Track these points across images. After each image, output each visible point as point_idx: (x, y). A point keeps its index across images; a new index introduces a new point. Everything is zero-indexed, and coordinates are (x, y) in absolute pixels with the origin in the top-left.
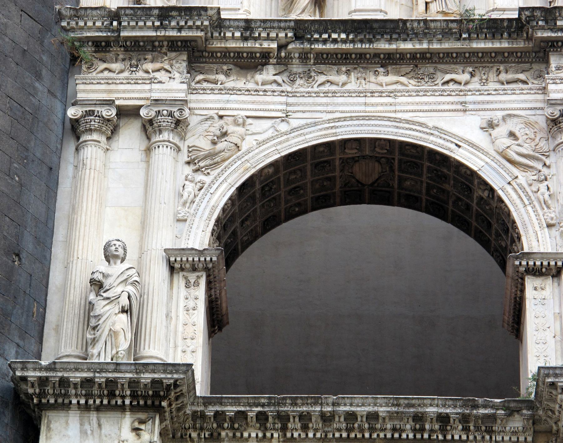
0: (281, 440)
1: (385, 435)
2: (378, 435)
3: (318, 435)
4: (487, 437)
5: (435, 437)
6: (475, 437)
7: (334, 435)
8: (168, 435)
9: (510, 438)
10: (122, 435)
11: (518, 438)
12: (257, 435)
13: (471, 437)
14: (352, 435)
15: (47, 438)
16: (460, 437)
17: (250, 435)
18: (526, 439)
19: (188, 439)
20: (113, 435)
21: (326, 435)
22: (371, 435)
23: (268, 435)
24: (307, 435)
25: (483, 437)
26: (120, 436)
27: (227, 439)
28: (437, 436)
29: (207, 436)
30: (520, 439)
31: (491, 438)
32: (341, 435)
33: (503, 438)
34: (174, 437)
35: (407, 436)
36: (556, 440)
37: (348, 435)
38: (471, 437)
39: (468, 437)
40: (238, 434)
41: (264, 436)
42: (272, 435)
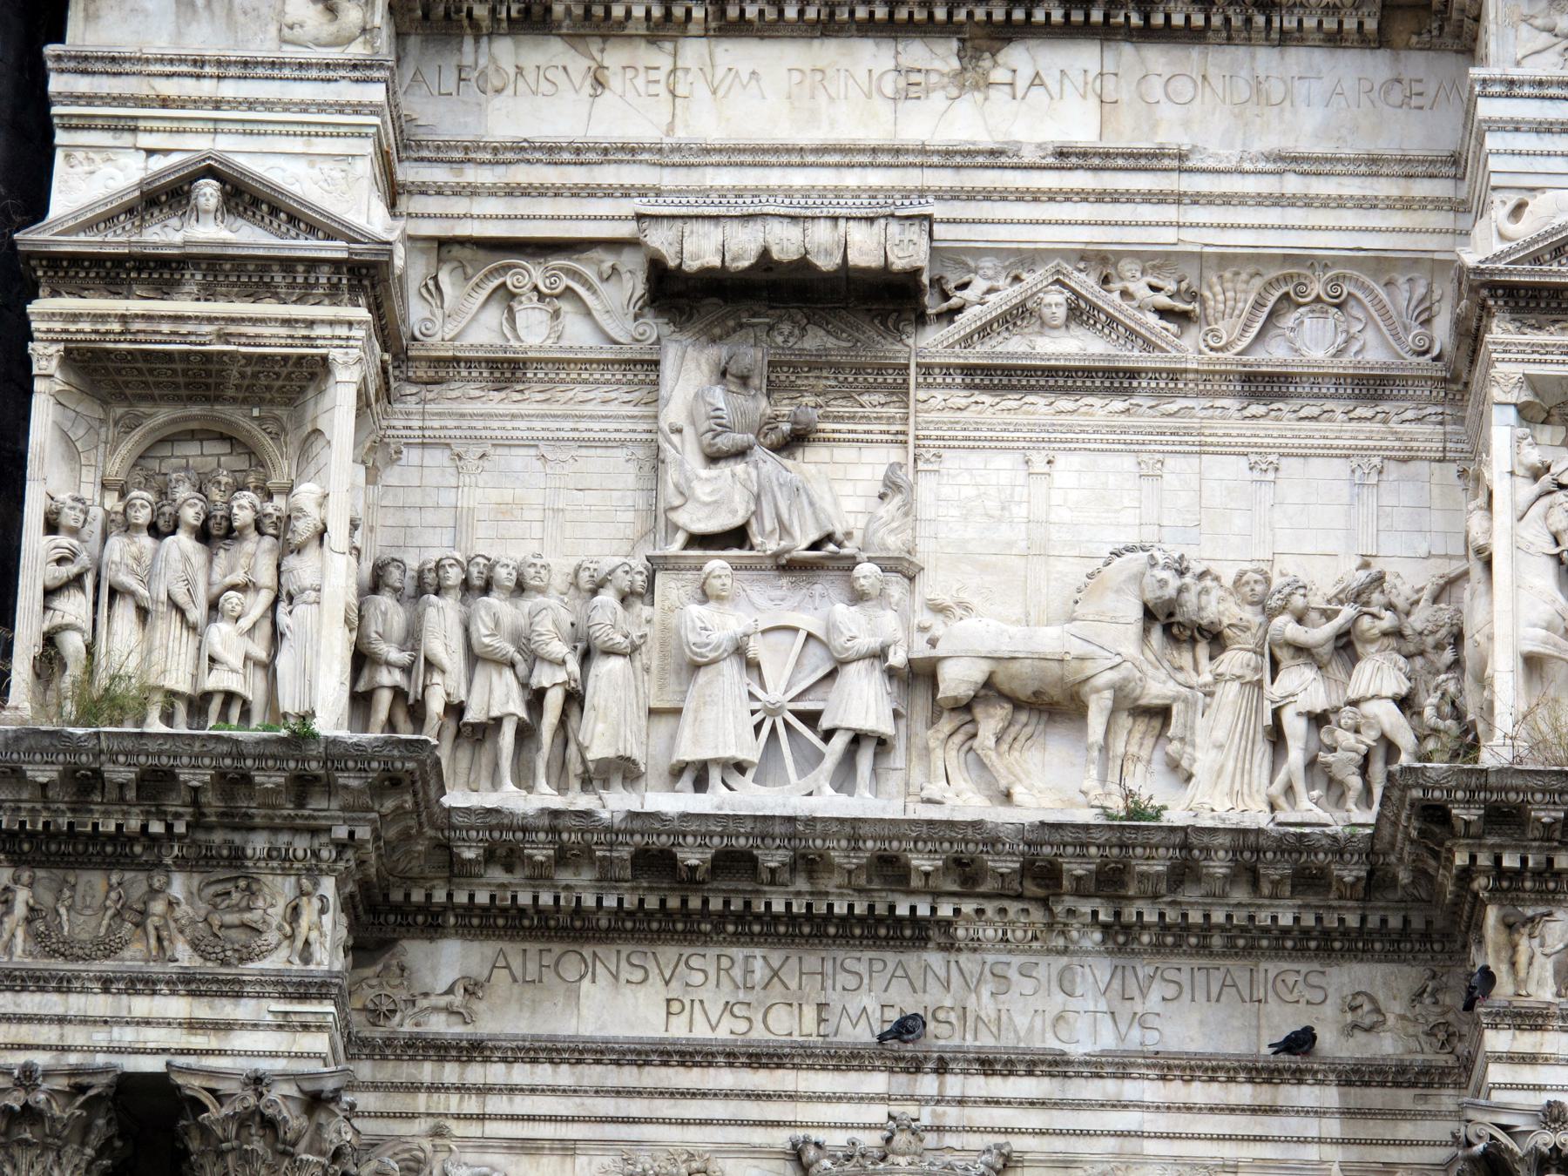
0: (713, 25)
1: (989, 15)
2: (970, 14)
3: (811, 13)
4: (1260, 20)
5: (1121, 19)
6: (1227, 20)
7: (852, 13)
8: (411, 10)
9: (1320, 23)
10: (288, 9)
11: (1340, 23)
12: (648, 12)
13: (1216, 21)
14: (902, 14)
15: (87, 18)
16: (1188, 18)
17: (628, 13)
18: (1361, 24)
19: (466, 23)
20: (264, 10)
21: (832, 14)
22: (950, 14)
23: (679, 12)
24: (781, 12)
25: (1248, 21)
26: (282, 12)
27: (567, 22)
28: (1127, 18)
29: (514, 14)
30: (1346, 26)
31: (1269, 22)
32: (872, 14)
33: (1300, 22)
34: (426, 16)
35: (1048, 15)
36: (1441, 28)
37: (891, 14)
38: (1216, 21)
39: (1208, 19)
40: (598, 11)
41: (668, 15)
42: (688, 12)
